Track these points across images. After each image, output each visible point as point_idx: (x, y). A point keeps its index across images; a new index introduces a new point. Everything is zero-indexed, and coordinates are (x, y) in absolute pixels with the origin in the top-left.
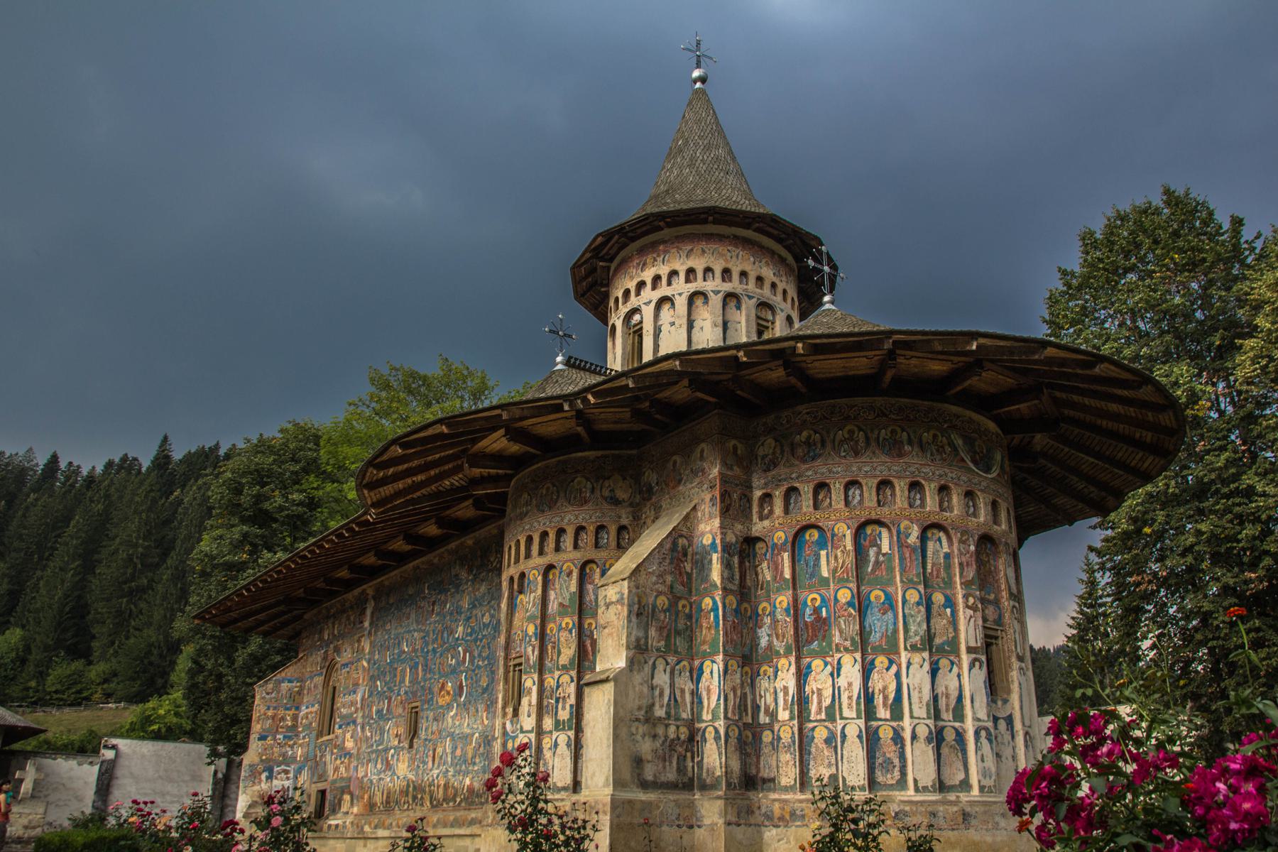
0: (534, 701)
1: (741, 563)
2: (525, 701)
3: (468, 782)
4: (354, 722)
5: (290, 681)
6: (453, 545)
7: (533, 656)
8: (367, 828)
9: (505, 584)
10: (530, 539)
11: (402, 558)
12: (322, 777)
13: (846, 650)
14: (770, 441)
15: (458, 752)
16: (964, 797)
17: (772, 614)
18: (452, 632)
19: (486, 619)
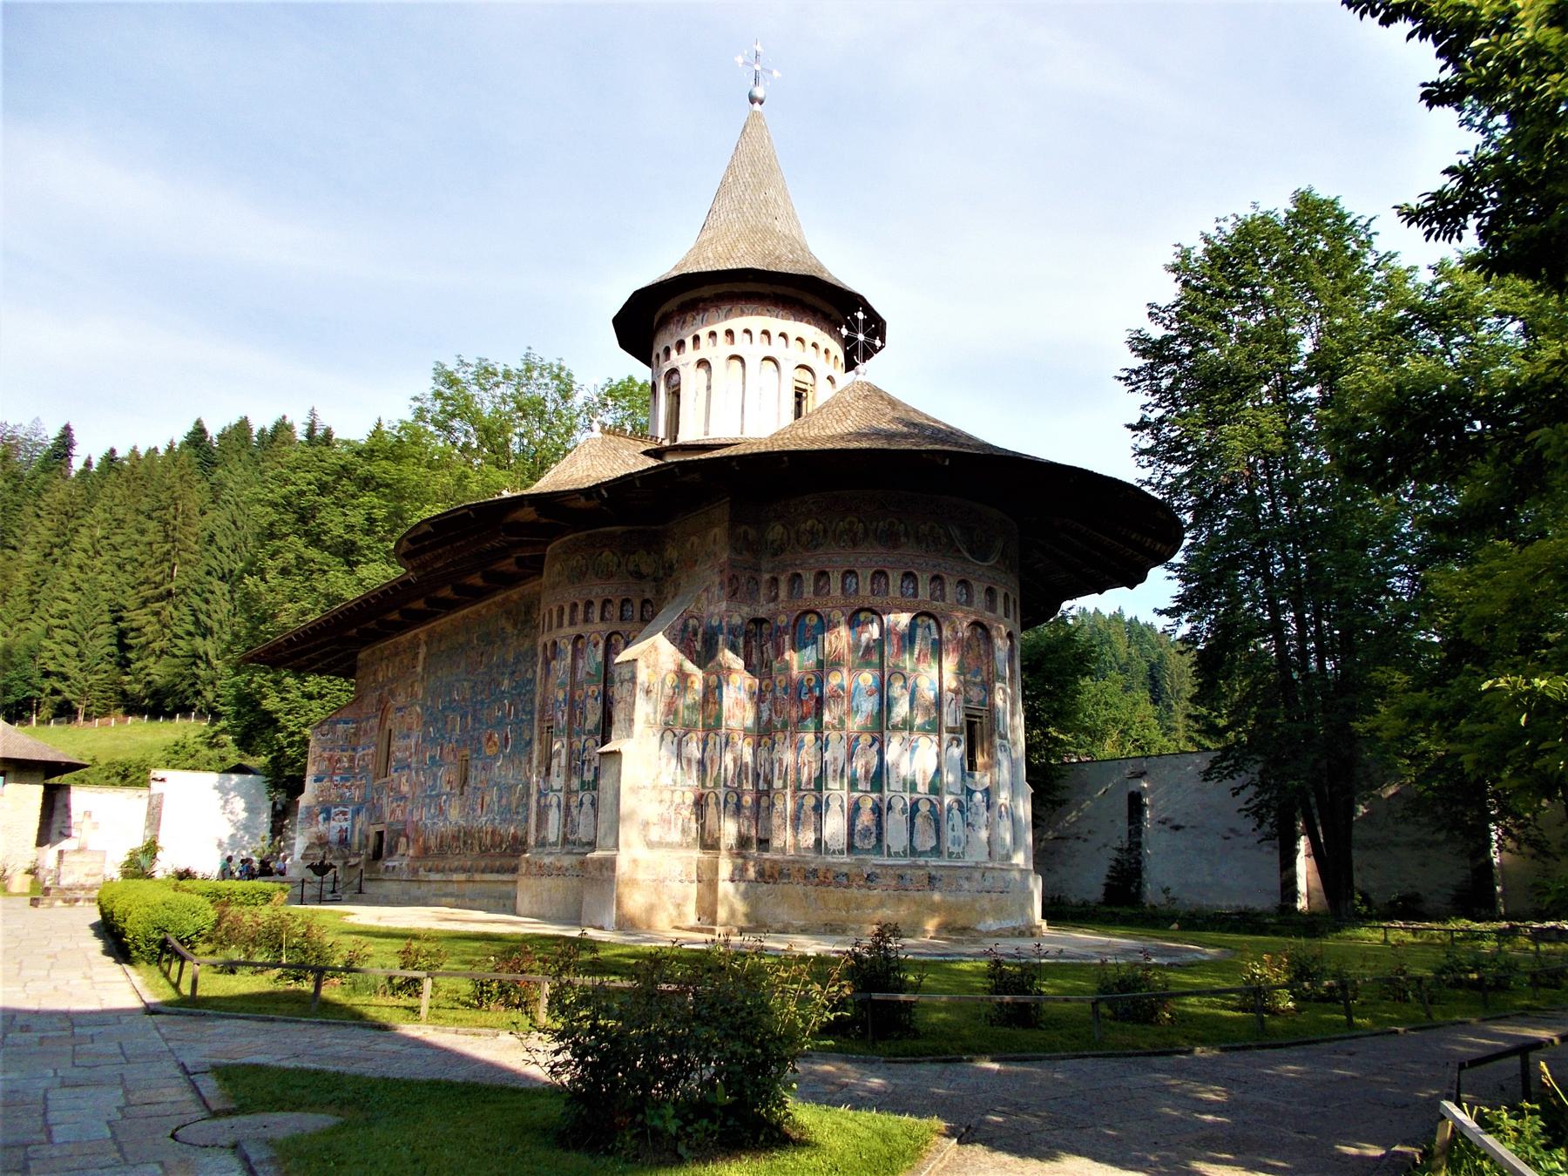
0: (563, 763)
1: (747, 643)
2: (555, 762)
3: (512, 830)
4: (409, 766)
5: (346, 723)
6: (498, 598)
7: (562, 719)
8: (421, 872)
9: (540, 649)
10: (561, 609)
11: (450, 606)
12: (380, 820)
13: (834, 727)
14: (779, 528)
15: (504, 801)
16: (933, 861)
17: (773, 691)
18: (499, 685)
19: (529, 675)
